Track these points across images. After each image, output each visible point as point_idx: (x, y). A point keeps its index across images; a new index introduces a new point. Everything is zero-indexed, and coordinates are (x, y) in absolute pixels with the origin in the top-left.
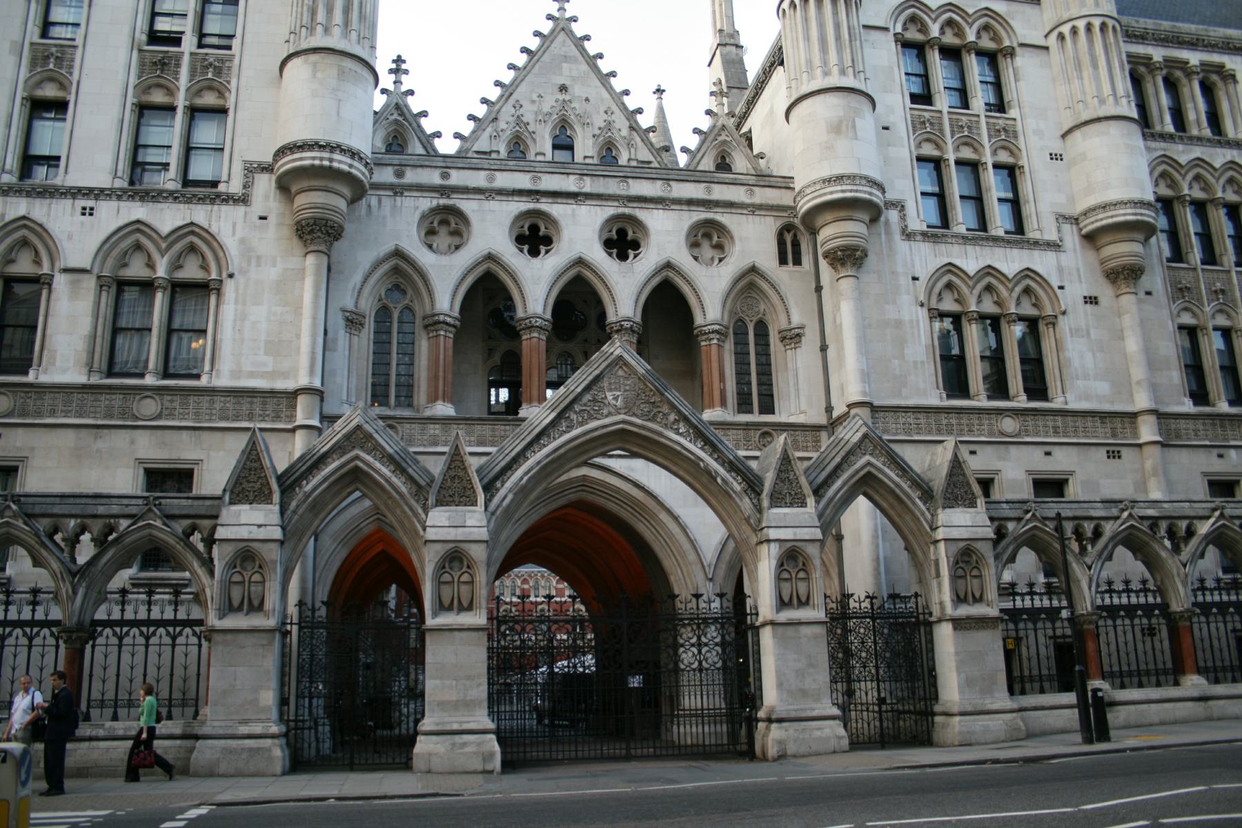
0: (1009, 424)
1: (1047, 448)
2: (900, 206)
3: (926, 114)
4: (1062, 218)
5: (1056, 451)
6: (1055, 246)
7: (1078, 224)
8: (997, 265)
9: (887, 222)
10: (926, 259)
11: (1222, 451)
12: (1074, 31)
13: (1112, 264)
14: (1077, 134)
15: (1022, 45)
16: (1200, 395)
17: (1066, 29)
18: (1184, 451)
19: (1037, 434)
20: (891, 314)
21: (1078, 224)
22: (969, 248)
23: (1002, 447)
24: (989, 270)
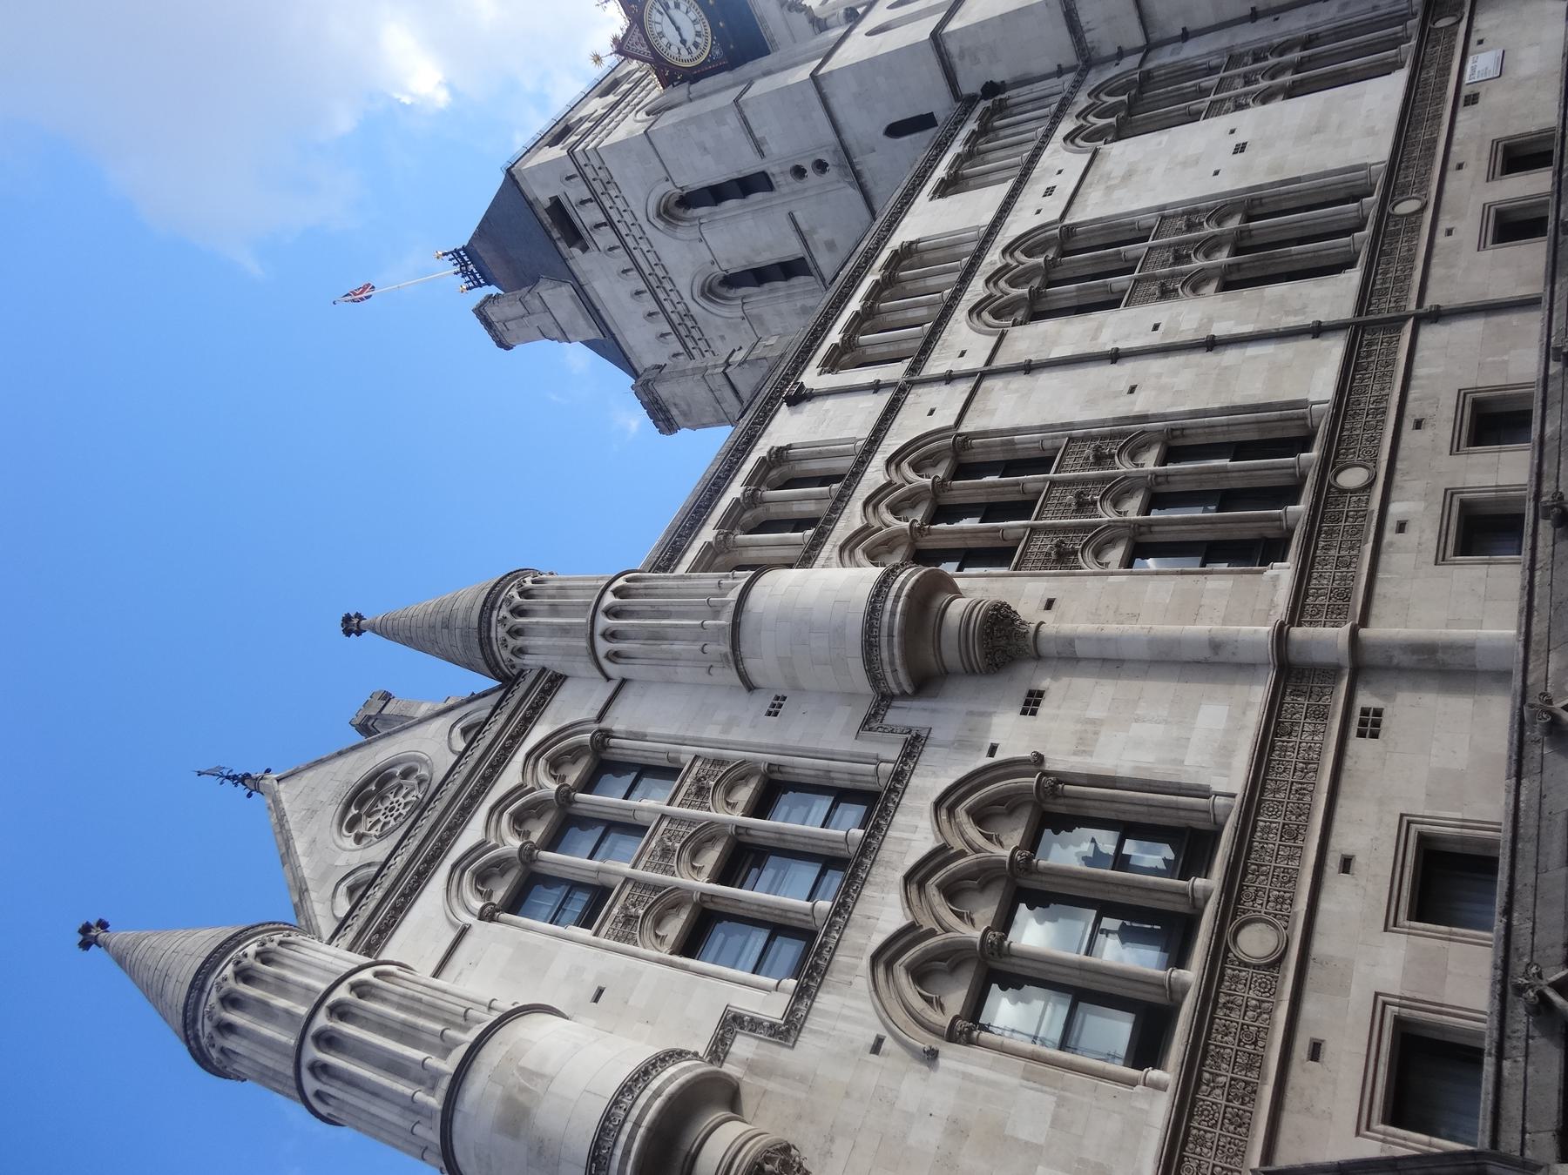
0: (1255, 942)
1: (1333, 863)
2: (733, 1023)
3: (615, 911)
4: (871, 722)
5: (1342, 842)
6: (914, 746)
7: (893, 697)
8: (910, 861)
9: (751, 1066)
10: (849, 1006)
11: (1391, 524)
12: (611, 635)
13: (977, 653)
14: (750, 664)
15: (600, 718)
16: (1266, 550)
17: (603, 647)
18: (1379, 589)
19: (1292, 878)
20: (928, 1136)
21: (893, 697)
22: (859, 911)
23: (1313, 972)
24: (916, 877)
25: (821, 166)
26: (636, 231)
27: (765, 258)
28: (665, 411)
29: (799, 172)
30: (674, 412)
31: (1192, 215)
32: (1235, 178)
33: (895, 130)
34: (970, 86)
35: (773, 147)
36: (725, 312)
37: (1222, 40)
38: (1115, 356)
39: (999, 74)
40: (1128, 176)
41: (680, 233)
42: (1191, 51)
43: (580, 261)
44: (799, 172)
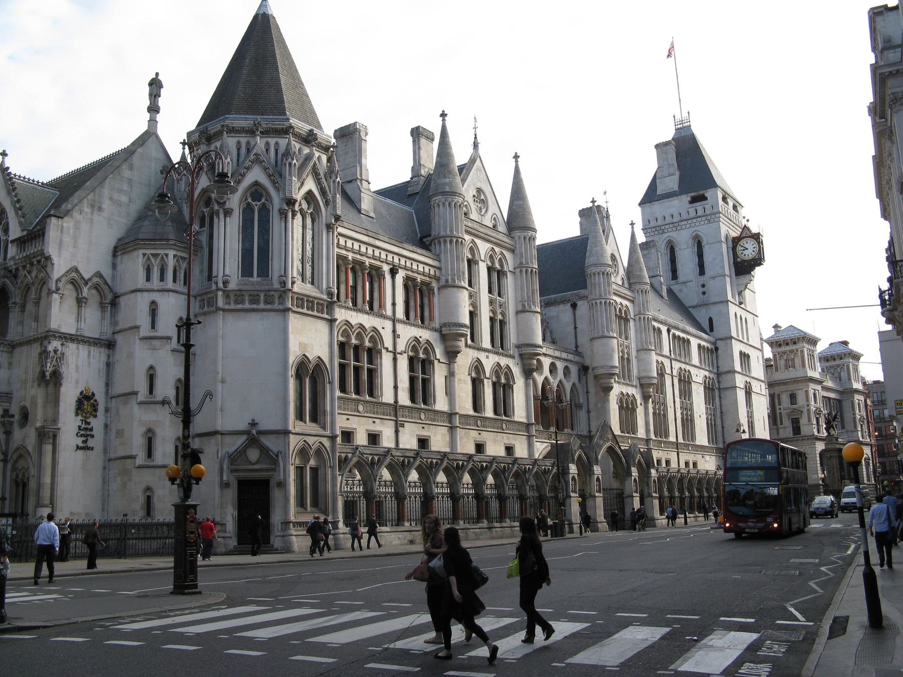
25: (704, 293)
26: (693, 225)
27: (679, 267)
28: (646, 249)
29: (703, 286)
30: (646, 252)
31: (692, 410)
32: (696, 416)
33: (711, 320)
34: (720, 344)
35: (712, 282)
36: (663, 246)
37: (718, 407)
38: (674, 402)
39: (720, 351)
40: (698, 393)
41: (690, 241)
42: (717, 399)
43: (686, 198)
44: (703, 286)
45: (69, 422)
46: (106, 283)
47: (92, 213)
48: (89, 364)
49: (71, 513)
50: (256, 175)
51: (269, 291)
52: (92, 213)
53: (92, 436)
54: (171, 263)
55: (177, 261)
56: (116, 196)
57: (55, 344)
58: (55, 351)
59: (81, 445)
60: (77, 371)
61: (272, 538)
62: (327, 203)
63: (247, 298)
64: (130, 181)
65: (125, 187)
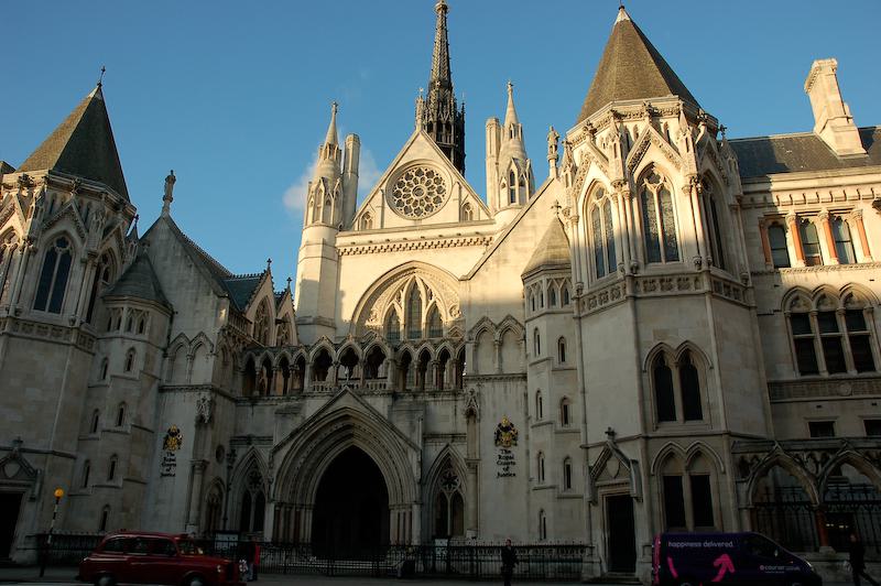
45: (490, 454)
46: (517, 323)
47: (498, 266)
48: (506, 397)
49: (496, 536)
50: (594, 172)
51: (613, 284)
52: (498, 266)
53: (514, 464)
54: (544, 288)
55: (552, 283)
56: (520, 245)
57: (472, 386)
58: (472, 392)
59: (502, 472)
60: (494, 406)
61: (637, 565)
62: (678, 167)
63: (597, 299)
64: (534, 227)
65: (530, 234)
